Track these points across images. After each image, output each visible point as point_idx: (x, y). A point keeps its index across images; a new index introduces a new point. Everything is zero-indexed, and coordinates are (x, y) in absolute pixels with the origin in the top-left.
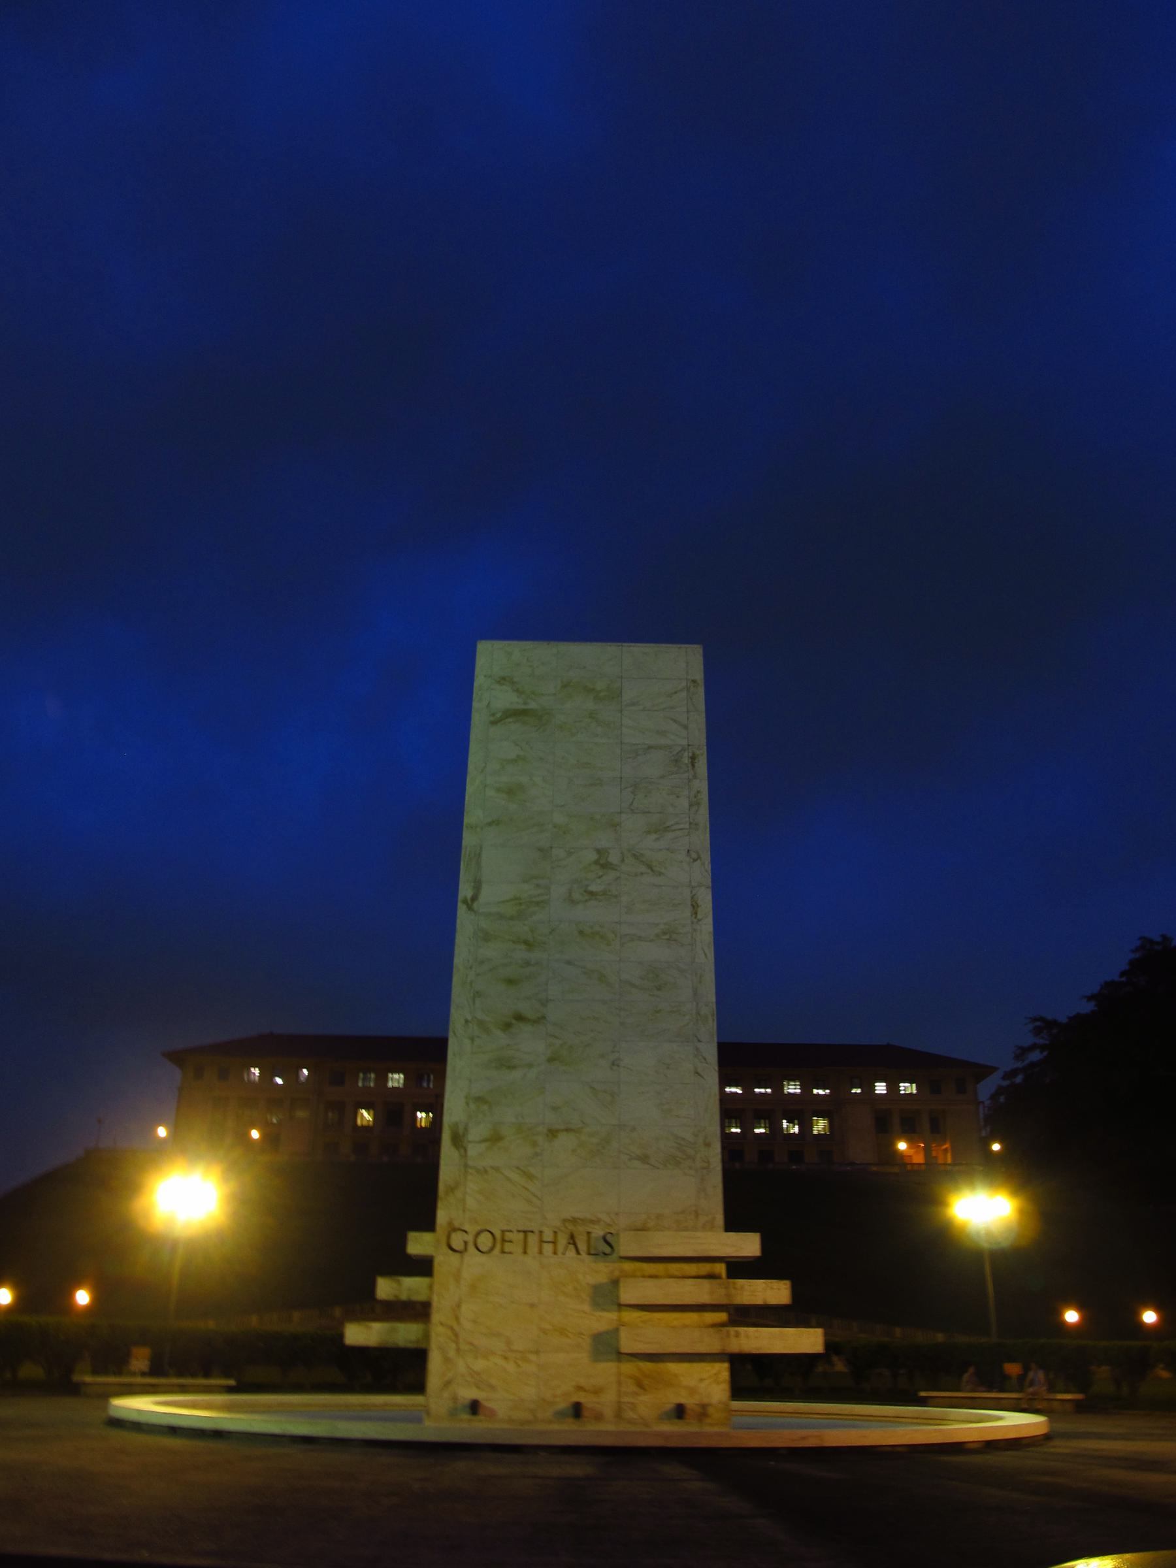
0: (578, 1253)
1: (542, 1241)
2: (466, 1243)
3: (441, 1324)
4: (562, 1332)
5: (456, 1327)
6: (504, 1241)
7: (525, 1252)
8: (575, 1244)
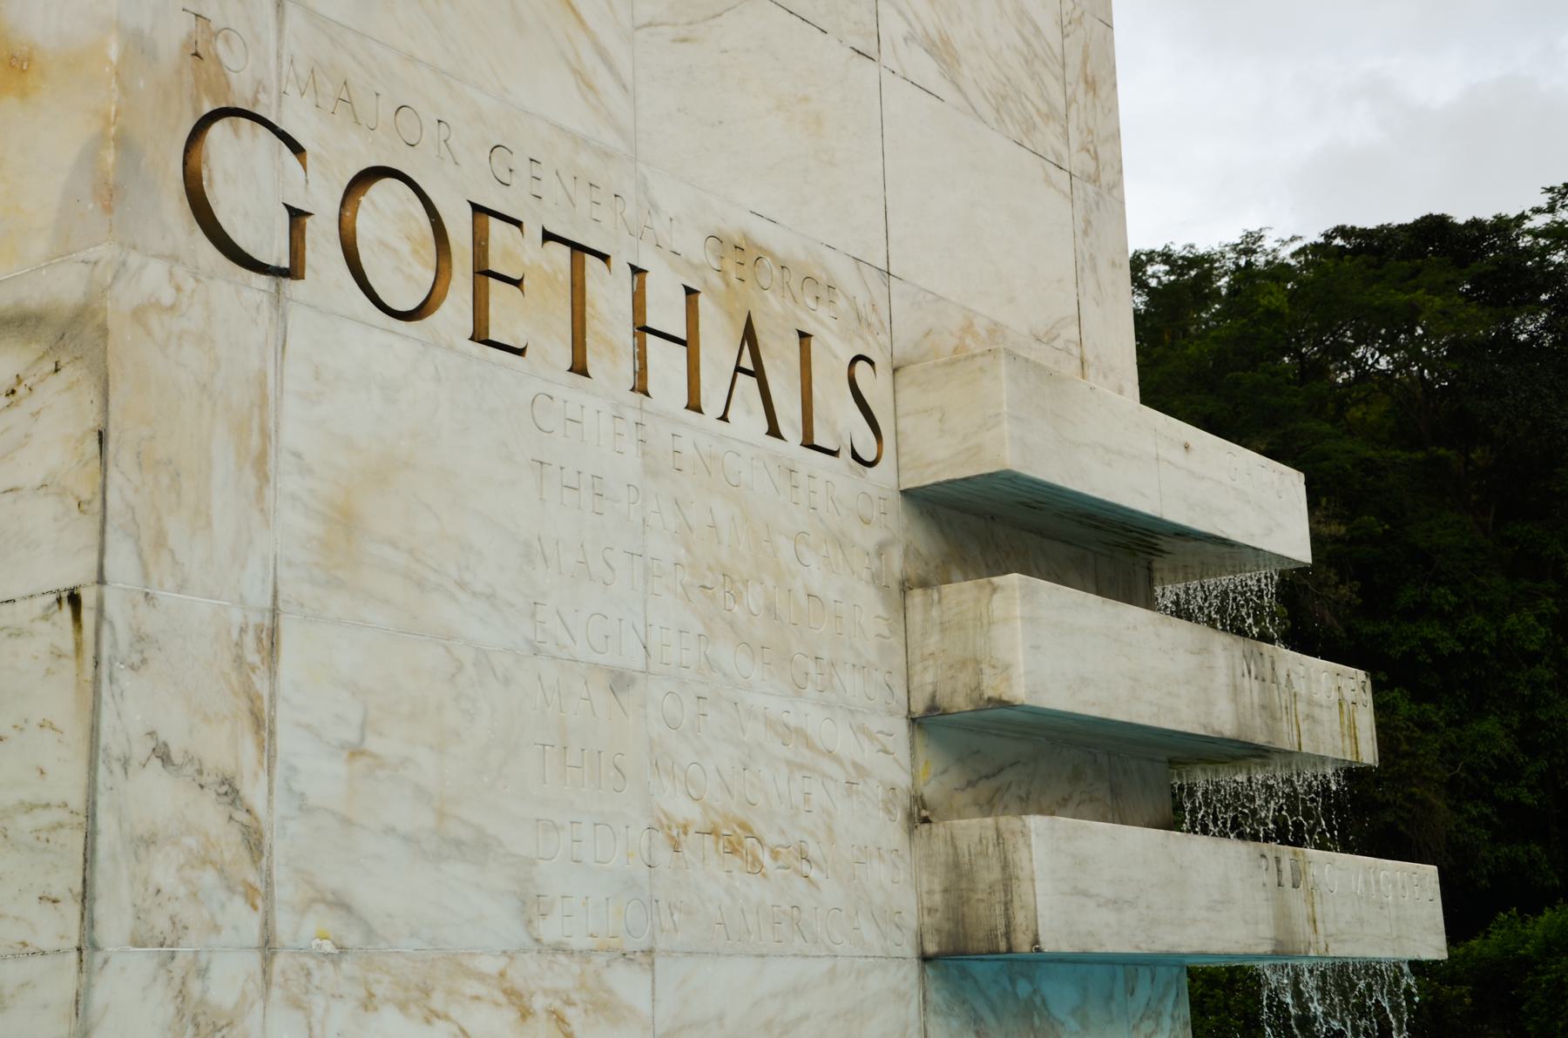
0: (774, 431)
1: (643, 329)
2: (297, 216)
3: (164, 756)
4: (734, 839)
5: (254, 793)
6: (483, 272)
7: (579, 368)
8: (758, 373)
